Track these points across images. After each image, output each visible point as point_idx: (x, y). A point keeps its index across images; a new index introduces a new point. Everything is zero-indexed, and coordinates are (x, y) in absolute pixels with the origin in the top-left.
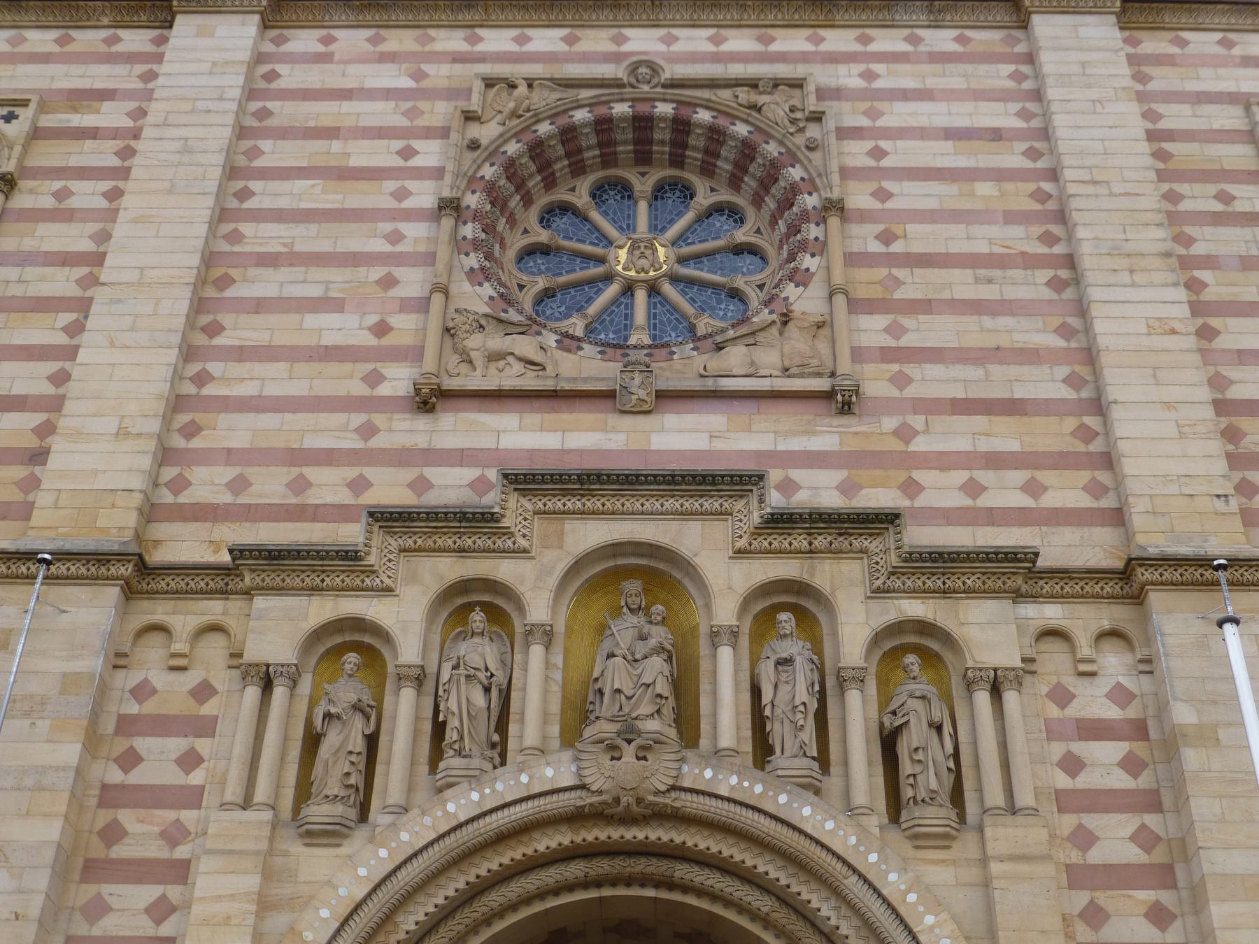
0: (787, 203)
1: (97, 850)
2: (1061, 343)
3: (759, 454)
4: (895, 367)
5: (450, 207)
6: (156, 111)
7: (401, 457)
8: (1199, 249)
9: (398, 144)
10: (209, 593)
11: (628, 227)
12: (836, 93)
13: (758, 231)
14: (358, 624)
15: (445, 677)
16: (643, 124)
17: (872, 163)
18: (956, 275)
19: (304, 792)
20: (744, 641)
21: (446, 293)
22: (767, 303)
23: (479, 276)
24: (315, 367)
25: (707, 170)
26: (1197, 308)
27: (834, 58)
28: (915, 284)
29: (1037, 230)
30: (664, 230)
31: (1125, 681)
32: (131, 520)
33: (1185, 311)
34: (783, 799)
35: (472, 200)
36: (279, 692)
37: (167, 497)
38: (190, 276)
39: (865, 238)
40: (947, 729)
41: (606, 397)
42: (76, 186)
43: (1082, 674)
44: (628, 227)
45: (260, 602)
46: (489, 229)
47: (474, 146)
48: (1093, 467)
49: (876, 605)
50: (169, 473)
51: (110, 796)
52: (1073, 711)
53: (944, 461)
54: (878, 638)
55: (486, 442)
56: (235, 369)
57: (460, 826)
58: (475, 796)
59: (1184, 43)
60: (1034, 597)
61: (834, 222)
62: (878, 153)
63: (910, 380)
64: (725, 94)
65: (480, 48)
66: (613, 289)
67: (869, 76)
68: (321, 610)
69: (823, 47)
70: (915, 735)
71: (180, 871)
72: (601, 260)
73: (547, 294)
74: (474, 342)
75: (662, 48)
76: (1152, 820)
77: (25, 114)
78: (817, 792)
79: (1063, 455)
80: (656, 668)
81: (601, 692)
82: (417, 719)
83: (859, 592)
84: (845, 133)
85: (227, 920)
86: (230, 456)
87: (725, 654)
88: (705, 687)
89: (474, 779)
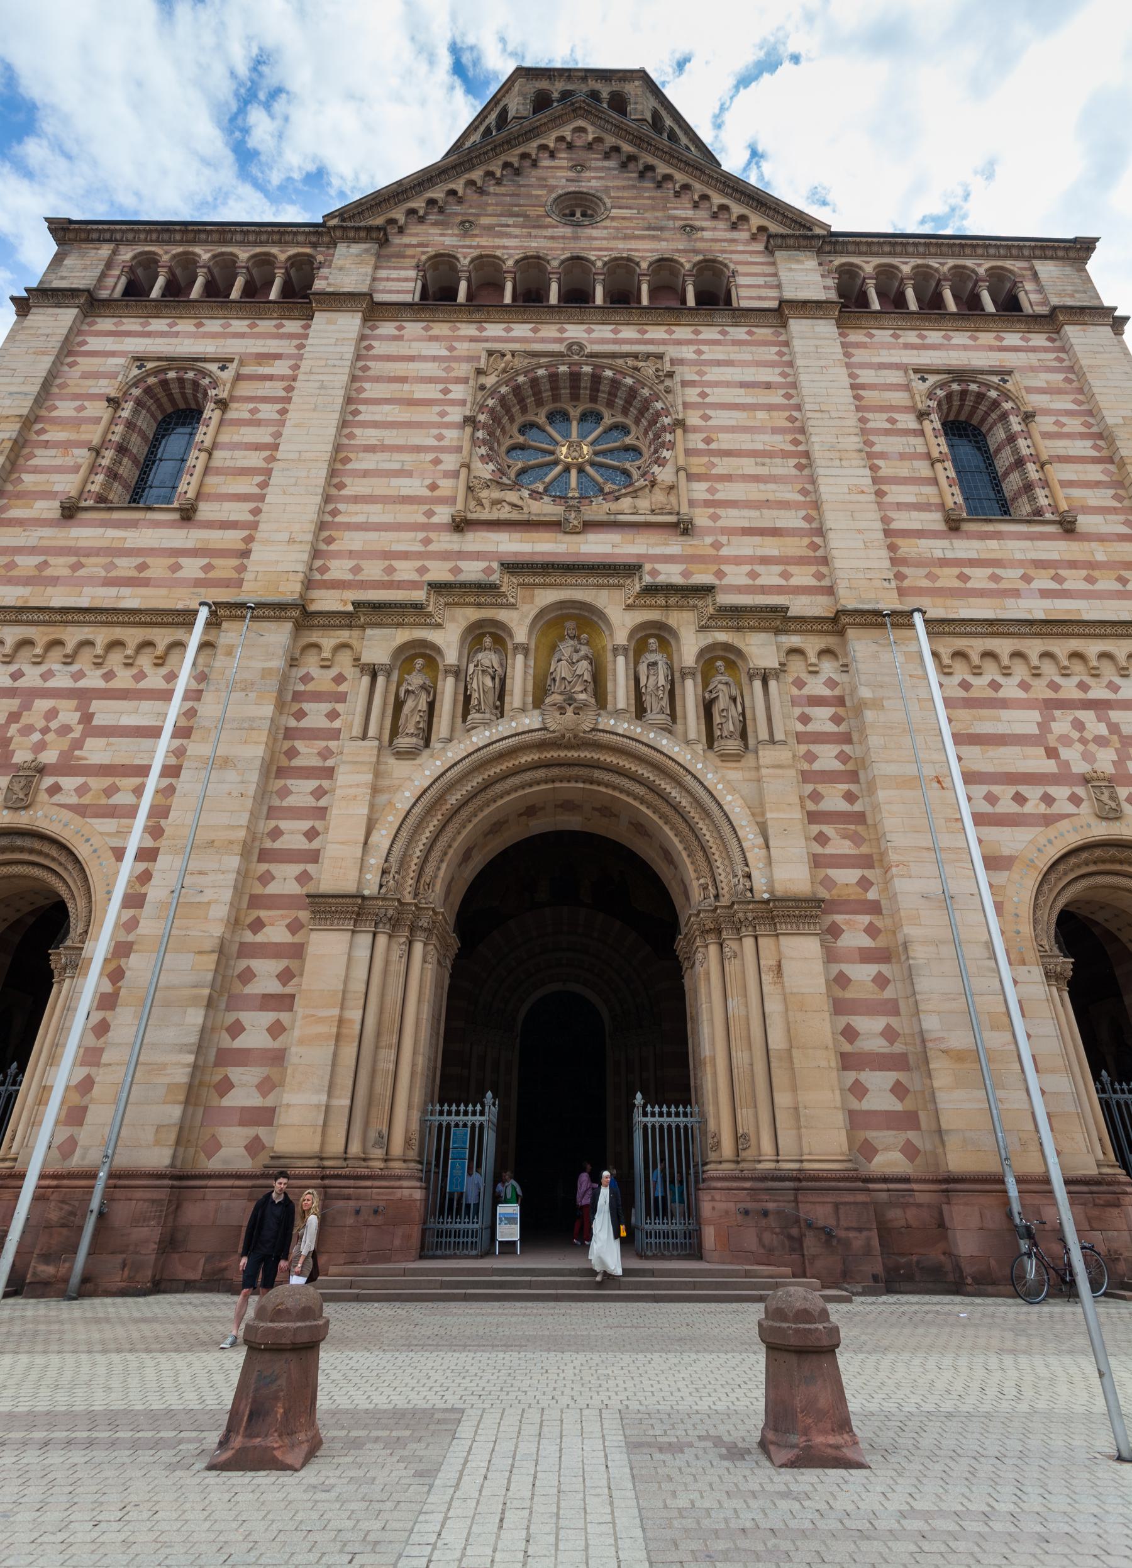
0: (653, 422)
1: (284, 762)
3: (639, 555)
4: (711, 510)
5: (470, 421)
6: (305, 365)
7: (445, 556)
8: (877, 448)
9: (441, 386)
10: (341, 627)
11: (566, 435)
12: (681, 362)
14: (424, 643)
15: (470, 671)
16: (575, 377)
17: (700, 400)
18: (745, 461)
19: (395, 732)
20: (631, 654)
22: (643, 475)
23: (485, 459)
24: (398, 507)
25: (610, 404)
26: (875, 481)
27: (679, 342)
28: (723, 466)
29: (789, 437)
30: (586, 437)
31: (834, 676)
32: (298, 587)
33: (869, 481)
34: (652, 735)
35: (482, 418)
36: (381, 680)
37: (318, 576)
38: (327, 456)
39: (696, 441)
40: (739, 700)
41: (555, 525)
42: (261, 406)
43: (811, 672)
45: (369, 632)
46: (491, 434)
47: (482, 387)
48: (818, 564)
49: (701, 635)
50: (318, 563)
52: (806, 691)
53: (738, 561)
54: (702, 653)
55: (491, 548)
56: (353, 508)
57: (479, 749)
58: (487, 733)
60: (786, 632)
61: (679, 432)
62: (703, 395)
63: (719, 517)
64: (620, 361)
65: (484, 334)
67: (699, 352)
68: (403, 636)
69: (674, 336)
70: (722, 702)
72: (552, 453)
73: (522, 472)
76: (847, 748)
77: (232, 367)
78: (670, 732)
79: (801, 557)
80: (583, 667)
81: (554, 680)
82: (456, 693)
83: (693, 628)
84: (685, 384)
85: (355, 798)
86: (351, 554)
87: (621, 660)
88: (610, 677)
89: (486, 724)
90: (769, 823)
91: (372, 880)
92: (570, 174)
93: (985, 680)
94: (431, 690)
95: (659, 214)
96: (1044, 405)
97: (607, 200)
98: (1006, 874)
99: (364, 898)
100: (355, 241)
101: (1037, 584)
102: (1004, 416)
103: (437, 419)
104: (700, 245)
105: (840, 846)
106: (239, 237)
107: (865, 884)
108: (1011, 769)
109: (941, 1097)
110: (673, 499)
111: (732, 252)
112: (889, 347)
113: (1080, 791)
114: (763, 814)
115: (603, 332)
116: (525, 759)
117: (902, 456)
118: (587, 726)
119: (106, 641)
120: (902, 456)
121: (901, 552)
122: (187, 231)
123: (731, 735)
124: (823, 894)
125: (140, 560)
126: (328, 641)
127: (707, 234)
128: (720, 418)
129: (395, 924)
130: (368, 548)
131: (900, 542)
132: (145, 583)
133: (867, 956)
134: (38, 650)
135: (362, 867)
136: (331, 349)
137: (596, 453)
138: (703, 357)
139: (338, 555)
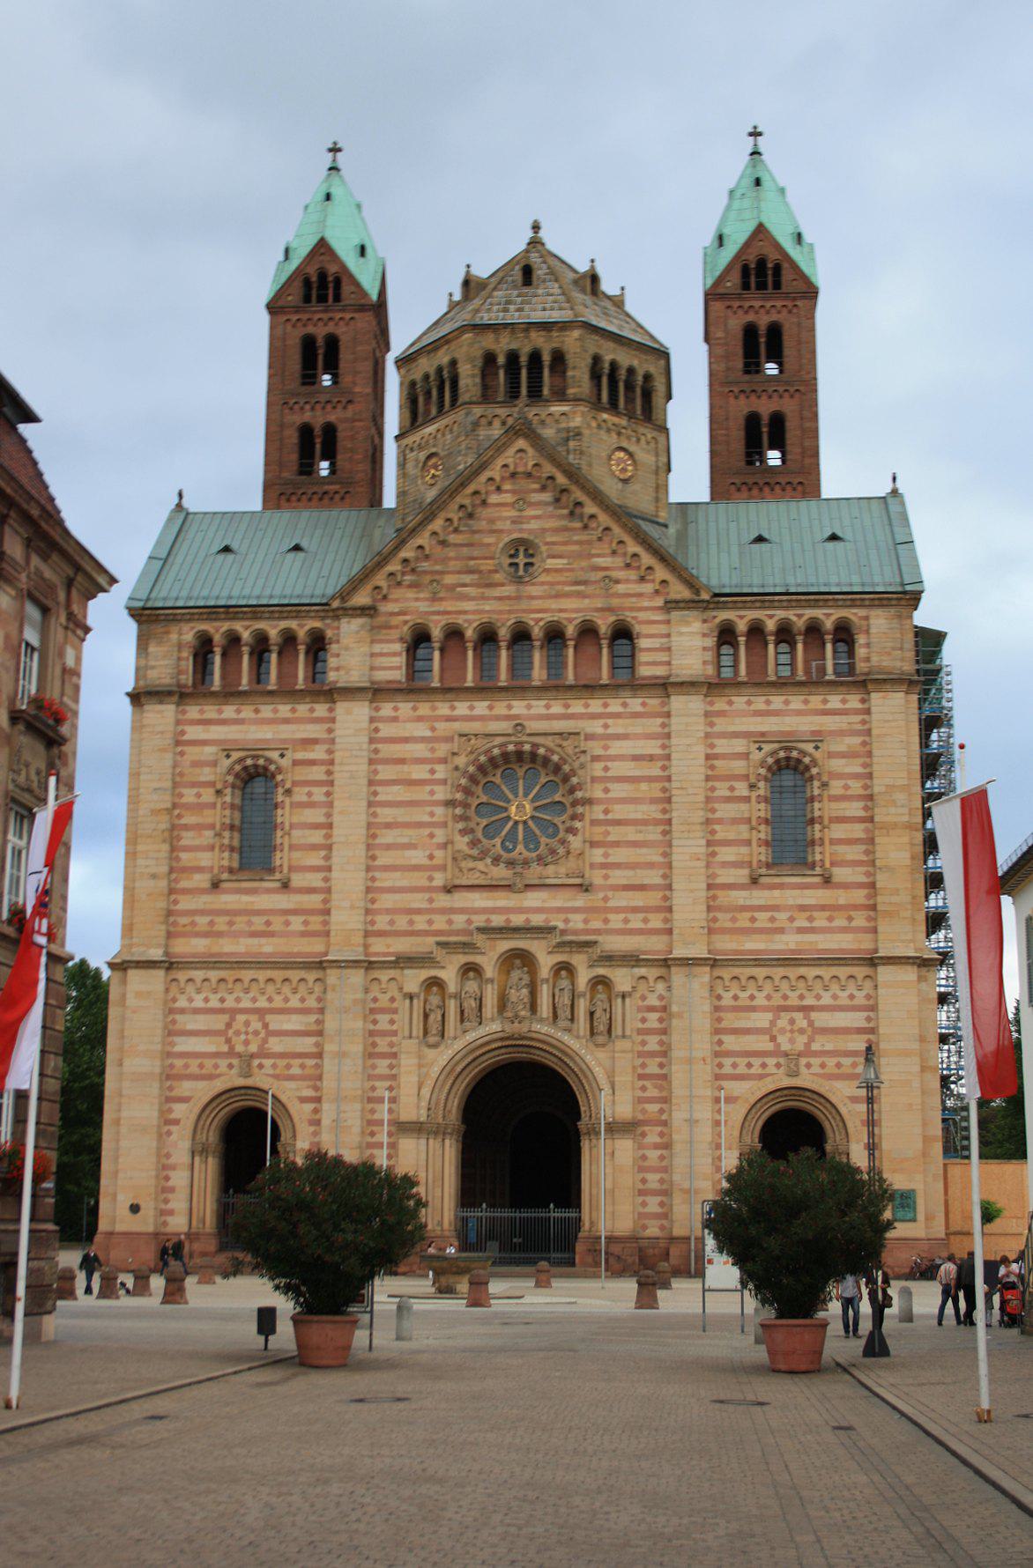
0: (572, 791)
4: (604, 871)
5: (450, 803)
7: (443, 911)
8: (718, 815)
9: (428, 767)
14: (435, 977)
17: (603, 774)
19: (426, 1033)
21: (452, 843)
23: (463, 832)
24: (411, 874)
28: (616, 833)
29: (660, 807)
36: (415, 1001)
37: (370, 928)
38: (363, 839)
39: (597, 812)
44: (516, 795)
47: (457, 768)
50: (369, 918)
51: (372, 1033)
53: (617, 910)
54: (590, 981)
59: (730, 703)
61: (587, 807)
62: (606, 769)
67: (606, 726)
69: (590, 710)
71: (394, 1055)
75: (524, 712)
76: (664, 1037)
77: (289, 754)
78: (570, 1031)
80: (525, 991)
83: (586, 965)
84: (596, 758)
86: (388, 911)
89: (474, 1029)
91: (424, 1112)
92: (513, 513)
94: (443, 1007)
95: (584, 564)
96: (840, 770)
97: (544, 548)
100: (353, 616)
101: (797, 924)
102: (811, 778)
103: (428, 797)
104: (615, 602)
105: (652, 1092)
106: (267, 615)
107: (662, 1111)
108: (747, 1049)
109: (675, 1208)
110: (580, 862)
112: (743, 714)
113: (782, 1060)
115: (538, 706)
117: (735, 821)
118: (525, 1030)
120: (735, 821)
122: (227, 613)
123: (601, 1034)
124: (640, 1117)
125: (265, 918)
126: (384, 976)
127: (621, 588)
129: (436, 1133)
131: (719, 893)
132: (272, 934)
133: (656, 1146)
134: (230, 986)
135: (418, 1107)
137: (536, 809)
138: (610, 731)
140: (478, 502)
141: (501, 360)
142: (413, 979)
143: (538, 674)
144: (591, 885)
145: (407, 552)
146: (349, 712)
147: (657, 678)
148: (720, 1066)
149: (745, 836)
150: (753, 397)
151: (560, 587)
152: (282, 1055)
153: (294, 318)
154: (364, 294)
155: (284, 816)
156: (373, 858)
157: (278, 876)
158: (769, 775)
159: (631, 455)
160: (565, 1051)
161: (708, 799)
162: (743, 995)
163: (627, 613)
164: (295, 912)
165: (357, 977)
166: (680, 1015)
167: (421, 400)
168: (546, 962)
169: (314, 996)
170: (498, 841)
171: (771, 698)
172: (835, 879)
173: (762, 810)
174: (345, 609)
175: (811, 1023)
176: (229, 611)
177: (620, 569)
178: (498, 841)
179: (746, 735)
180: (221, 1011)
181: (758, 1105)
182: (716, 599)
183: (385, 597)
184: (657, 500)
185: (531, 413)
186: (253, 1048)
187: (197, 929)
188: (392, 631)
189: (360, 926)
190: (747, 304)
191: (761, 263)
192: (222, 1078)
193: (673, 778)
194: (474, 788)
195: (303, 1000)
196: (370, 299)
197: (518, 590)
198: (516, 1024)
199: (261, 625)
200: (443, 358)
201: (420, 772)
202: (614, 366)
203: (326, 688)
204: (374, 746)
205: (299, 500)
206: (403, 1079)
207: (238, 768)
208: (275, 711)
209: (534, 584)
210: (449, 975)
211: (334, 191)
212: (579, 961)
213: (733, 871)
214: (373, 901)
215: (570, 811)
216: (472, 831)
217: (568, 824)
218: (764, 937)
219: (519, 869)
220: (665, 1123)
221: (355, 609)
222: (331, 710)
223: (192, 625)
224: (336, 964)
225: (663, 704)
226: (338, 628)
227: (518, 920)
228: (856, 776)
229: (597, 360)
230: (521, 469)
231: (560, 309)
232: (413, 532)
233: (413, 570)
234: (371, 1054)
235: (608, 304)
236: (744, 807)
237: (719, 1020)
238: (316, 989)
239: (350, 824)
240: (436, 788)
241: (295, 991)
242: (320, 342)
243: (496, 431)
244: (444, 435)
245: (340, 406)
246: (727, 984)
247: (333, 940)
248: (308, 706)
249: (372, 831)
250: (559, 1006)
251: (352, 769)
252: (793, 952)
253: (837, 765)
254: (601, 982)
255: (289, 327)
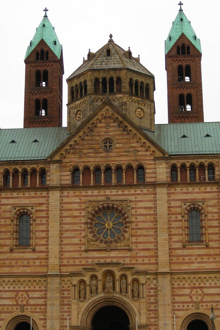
0: (125, 219)
2: (154, 241)
4: (136, 245)
5: (86, 223)
7: (84, 258)
8: (172, 226)
9: (79, 212)
10: (68, 277)
13: (122, 220)
14: (82, 279)
16: (108, 207)
19: (80, 297)
20: (120, 280)
21: (87, 236)
23: (91, 233)
24: (74, 246)
28: (139, 232)
29: (154, 224)
31: (155, 283)
37: (61, 264)
39: (134, 226)
41: (105, 250)
45: (73, 278)
47: (88, 212)
50: (61, 261)
51: (62, 298)
52: (150, 287)
53: (140, 257)
54: (132, 280)
56: (66, 247)
59: (175, 190)
60: (147, 275)
61: (130, 224)
62: (136, 212)
66: (106, 229)
67: (136, 198)
68: (79, 278)
69: (130, 193)
71: (70, 305)
74: (91, 243)
75: (110, 194)
76: (156, 298)
77: (34, 208)
80: (111, 283)
85: (75, 310)
86: (67, 258)
87: (118, 282)
88: (116, 284)
89: (95, 296)
90: (141, 313)
91: (79, 323)
92: (105, 130)
93: (183, 283)
95: (128, 146)
97: (115, 141)
98: (178, 319)
99: (79, 326)
100: (54, 163)
102: (202, 214)
103: (79, 222)
104: (138, 158)
105: (153, 315)
106: (27, 163)
107: (156, 321)
110: (128, 242)
111: (146, 160)
112: (180, 193)
113: (194, 304)
114: (140, 311)
115: (114, 192)
116: (102, 301)
117: (178, 228)
118: (111, 296)
119: (28, 281)
120: (178, 228)
121: (173, 254)
122: (14, 163)
123: (136, 297)
124: (149, 323)
125: (28, 261)
126: (66, 279)
127: (140, 153)
128: (140, 218)
130: (70, 257)
131: (173, 251)
134: (17, 283)
135: (78, 321)
136: (55, 203)
137: (113, 225)
138: (137, 199)
139: (64, 258)
140: (94, 126)
141: (101, 80)
142: (75, 280)
143: (114, 181)
144: (132, 249)
145: (71, 143)
146: (53, 194)
147: (152, 182)
148: (174, 306)
149: (181, 232)
150: (181, 89)
151: (120, 153)
152: (34, 305)
153: (33, 65)
154: (56, 57)
155: (33, 228)
156: (62, 241)
157: (31, 247)
158: (188, 213)
159: (142, 110)
160: (124, 302)
161: (169, 221)
162: (181, 284)
163: (142, 161)
164: (37, 259)
165: (57, 280)
166: (161, 290)
167: (75, 93)
168: (118, 274)
169: (44, 286)
170: (101, 235)
171: (188, 188)
172: (210, 246)
173: (186, 224)
174: (52, 161)
175: (203, 292)
176: (15, 162)
177: (140, 147)
178: (101, 235)
179: (181, 200)
180: (14, 291)
181: (187, 319)
182: (170, 157)
183: (64, 157)
184: (151, 124)
185: (110, 97)
186: (24, 303)
187: (6, 265)
188: (67, 168)
189: (58, 263)
190: (179, 59)
191: (183, 46)
192: (15, 313)
193: (158, 214)
194: (94, 218)
195: (40, 287)
196: (58, 59)
197: (107, 154)
198: (109, 294)
199: (25, 166)
200: (82, 79)
201: (76, 213)
202: (137, 81)
203: (46, 186)
204: (61, 205)
205: (35, 124)
206: (73, 312)
207: (18, 212)
208: (30, 194)
209: (112, 152)
210: (87, 279)
211: (45, 24)
212: (128, 273)
213: (177, 244)
214: (62, 255)
215: (125, 225)
216: (94, 232)
217: (124, 229)
218: (187, 265)
219: (109, 244)
220: (157, 325)
221: (55, 161)
222: (48, 194)
223: (3, 167)
224: (50, 276)
225: (154, 191)
226: (50, 167)
227: (109, 261)
228: (216, 213)
229: (131, 80)
230: (107, 116)
231: (119, 64)
232: (73, 136)
233: (73, 148)
234: (62, 304)
235: (134, 61)
236: (180, 223)
237: (174, 292)
238: (44, 284)
239: (54, 230)
240: (82, 218)
241: (37, 284)
242: (42, 72)
243: (99, 103)
244: (82, 104)
245: (48, 93)
246: (176, 280)
247: (49, 268)
248: (40, 193)
249: (61, 233)
250: (122, 288)
251: (55, 213)
252: (197, 269)
253: (210, 209)
254: (136, 281)
255: (32, 68)
